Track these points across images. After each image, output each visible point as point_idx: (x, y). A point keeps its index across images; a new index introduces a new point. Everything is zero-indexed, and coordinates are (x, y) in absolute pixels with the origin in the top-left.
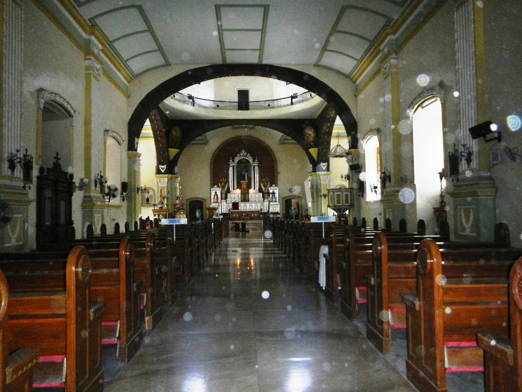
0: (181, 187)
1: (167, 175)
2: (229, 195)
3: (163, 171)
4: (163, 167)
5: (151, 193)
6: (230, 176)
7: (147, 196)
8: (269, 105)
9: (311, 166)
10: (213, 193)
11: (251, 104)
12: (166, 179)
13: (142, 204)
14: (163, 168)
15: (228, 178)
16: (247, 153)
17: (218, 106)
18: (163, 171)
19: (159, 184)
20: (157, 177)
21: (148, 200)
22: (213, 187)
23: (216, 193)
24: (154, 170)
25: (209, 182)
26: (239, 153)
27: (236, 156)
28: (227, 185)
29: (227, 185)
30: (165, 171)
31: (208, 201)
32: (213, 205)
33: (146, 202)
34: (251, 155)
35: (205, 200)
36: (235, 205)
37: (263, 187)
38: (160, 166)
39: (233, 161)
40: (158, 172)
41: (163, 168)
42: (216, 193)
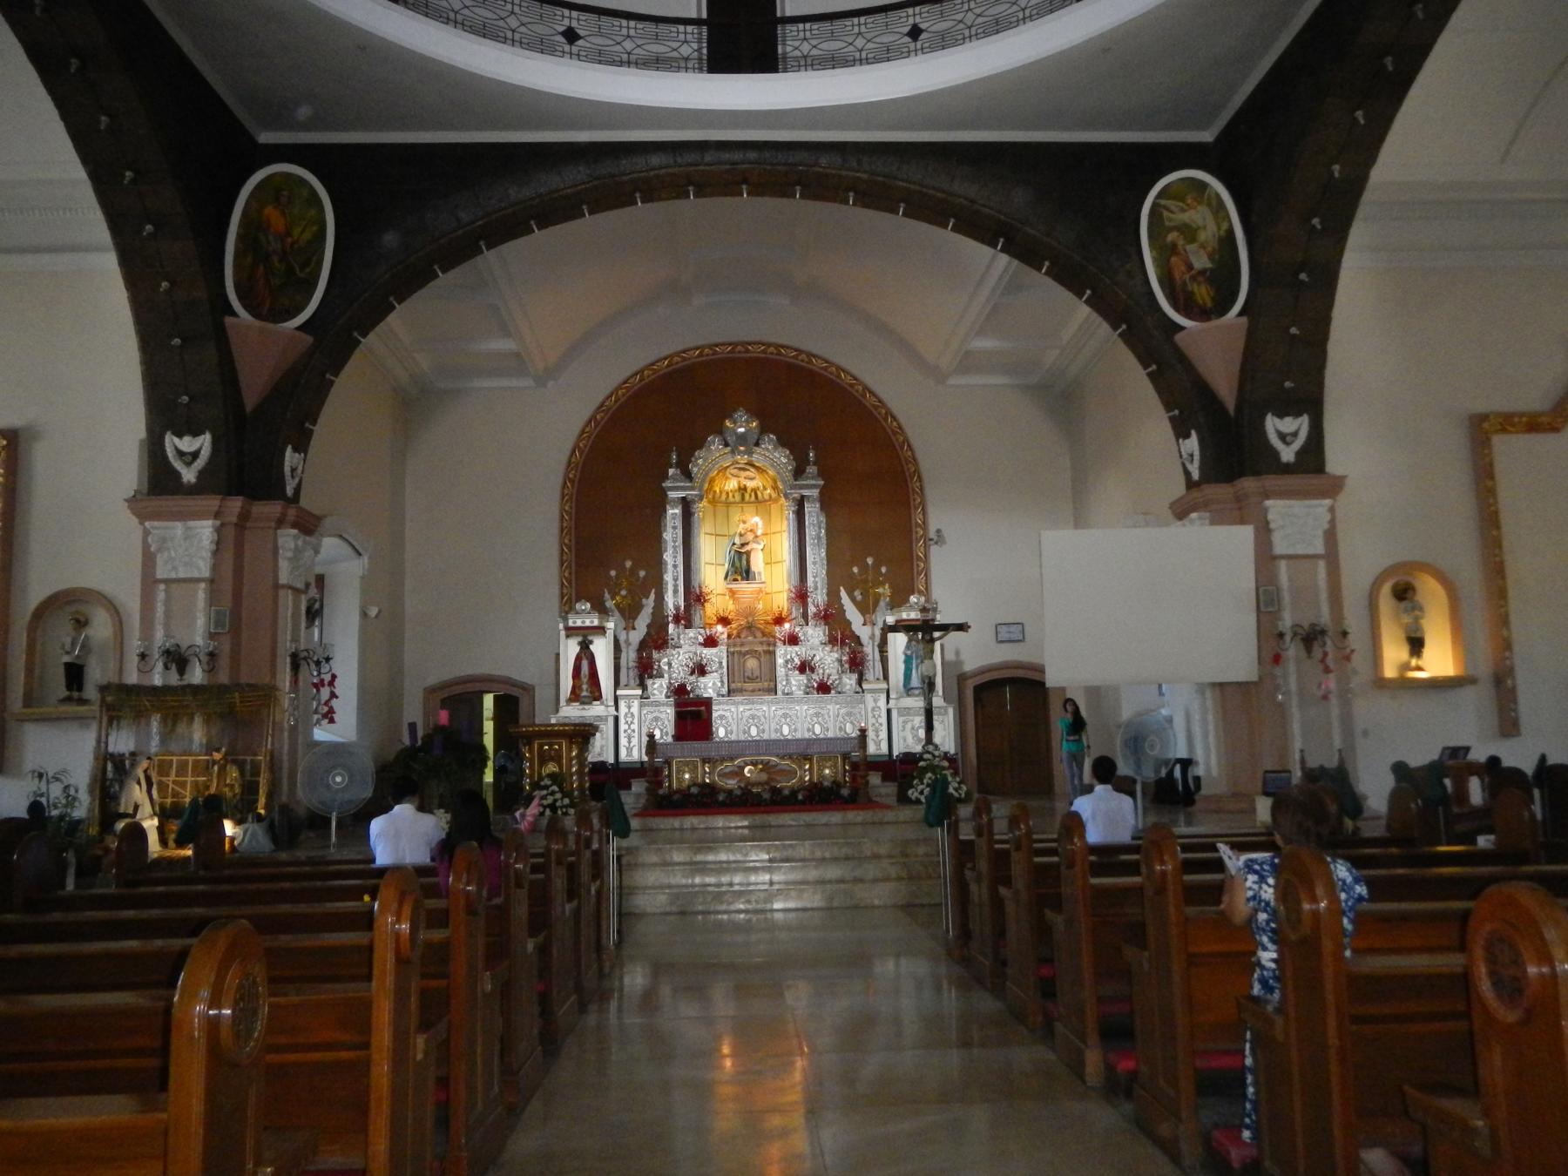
0: (373, 612)
1: (213, 502)
2: (663, 660)
3: (189, 475)
4: (187, 444)
5: (101, 628)
6: (668, 557)
7: (59, 646)
8: (915, 33)
9: (1192, 444)
10: (571, 649)
11: (791, 42)
12: (205, 530)
13: (29, 700)
14: (193, 449)
15: (657, 566)
16: (764, 430)
17: (571, 36)
18: (189, 475)
19: (160, 560)
20: (143, 517)
21: (75, 675)
22: (567, 607)
23: (585, 645)
24: (128, 471)
25: (556, 590)
26: (720, 431)
27: (701, 444)
28: (649, 603)
29: (649, 603)
30: (201, 474)
31: (542, 696)
32: (572, 712)
33: (63, 692)
34: (783, 442)
35: (528, 689)
36: (693, 717)
37: (853, 614)
38: (172, 442)
39: (688, 475)
40: (160, 480)
41: (193, 449)
42: (585, 645)
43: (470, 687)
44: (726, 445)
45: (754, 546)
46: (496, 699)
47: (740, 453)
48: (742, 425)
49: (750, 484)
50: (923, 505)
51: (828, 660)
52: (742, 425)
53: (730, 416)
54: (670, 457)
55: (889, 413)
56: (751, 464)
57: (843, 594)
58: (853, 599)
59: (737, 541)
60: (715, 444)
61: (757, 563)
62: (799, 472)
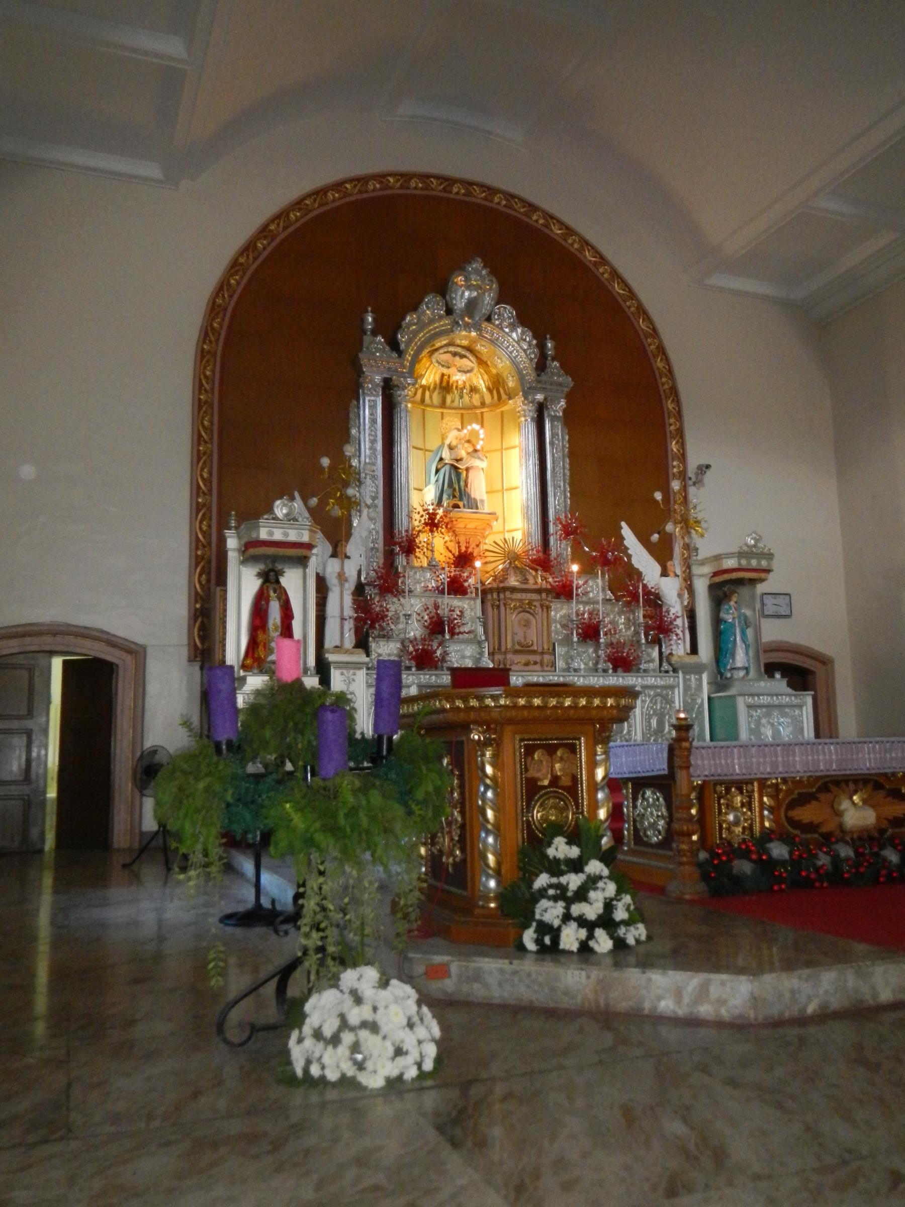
26: (443, 289)
34: (523, 320)
43: (32, 644)
44: (449, 311)
45: (477, 463)
46: (66, 663)
47: (467, 327)
48: (470, 286)
49: (459, 378)
50: (680, 433)
51: (621, 624)
52: (470, 286)
53: (459, 266)
54: (363, 321)
55: (642, 311)
56: (469, 349)
57: (626, 531)
58: (644, 539)
59: (446, 454)
60: (431, 307)
61: (478, 487)
62: (541, 367)
